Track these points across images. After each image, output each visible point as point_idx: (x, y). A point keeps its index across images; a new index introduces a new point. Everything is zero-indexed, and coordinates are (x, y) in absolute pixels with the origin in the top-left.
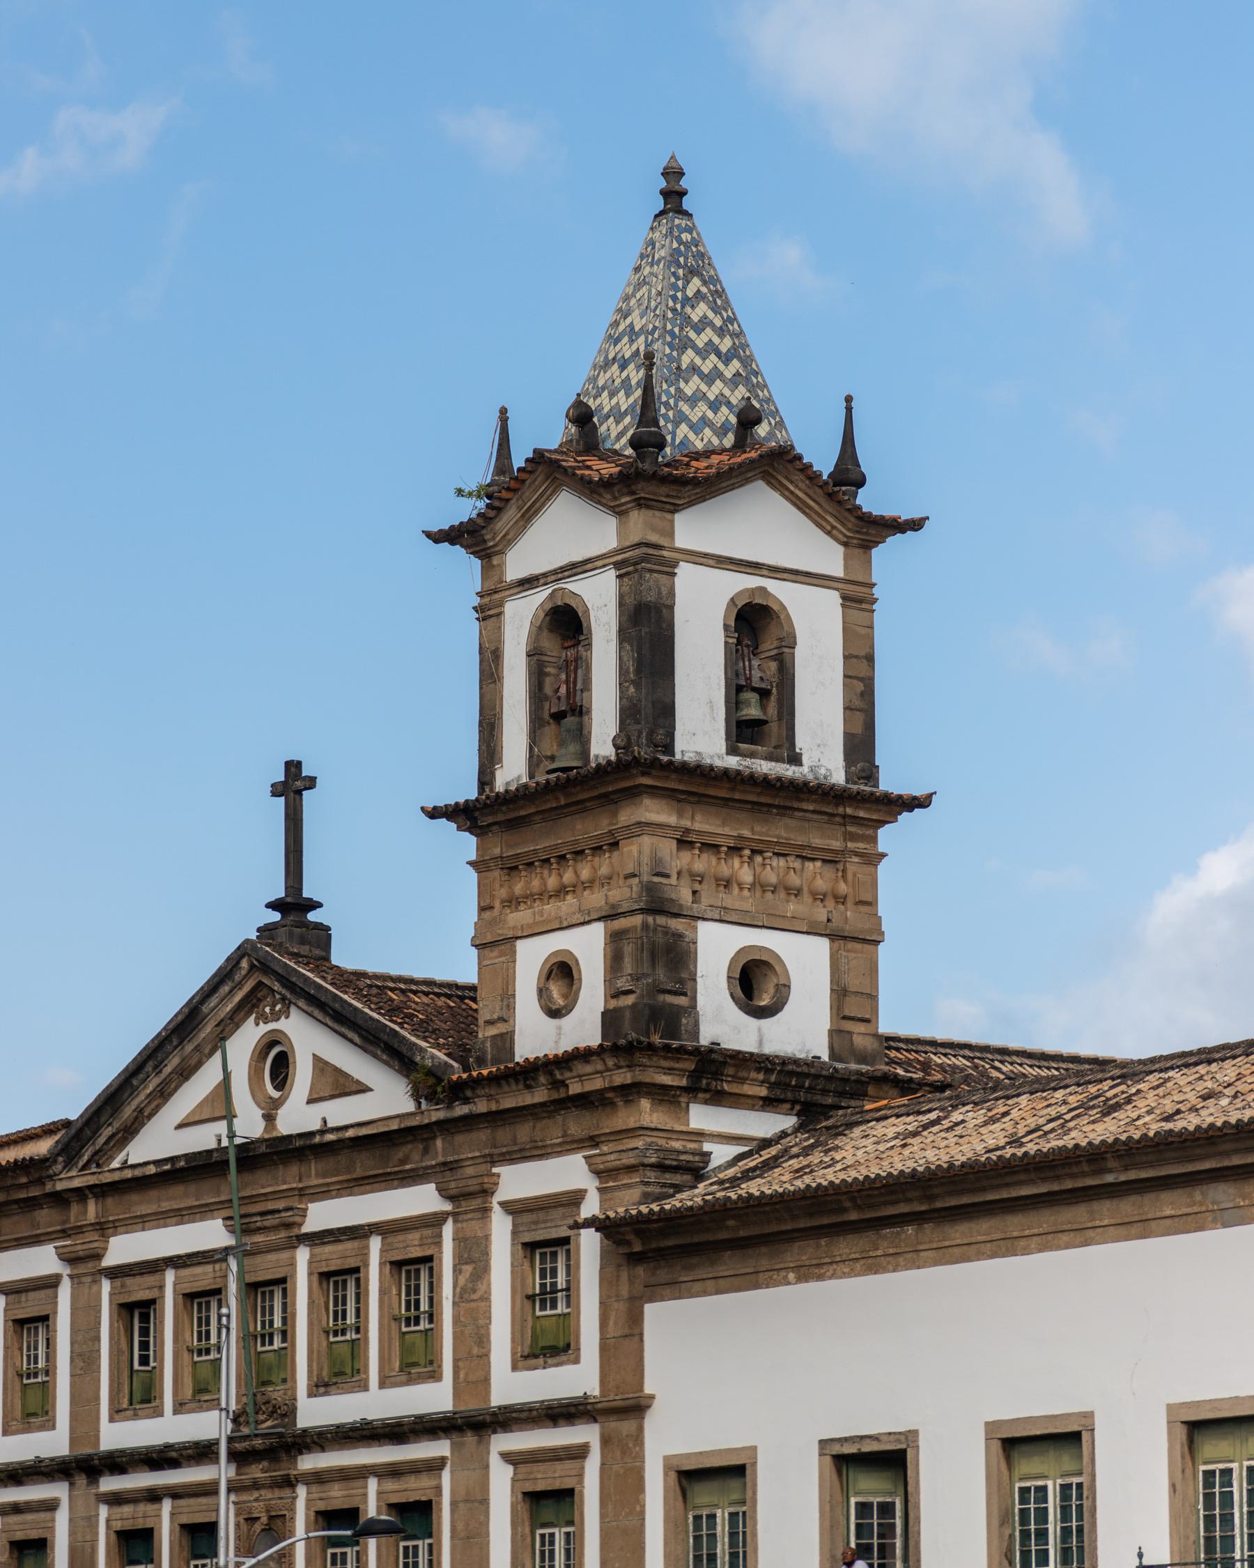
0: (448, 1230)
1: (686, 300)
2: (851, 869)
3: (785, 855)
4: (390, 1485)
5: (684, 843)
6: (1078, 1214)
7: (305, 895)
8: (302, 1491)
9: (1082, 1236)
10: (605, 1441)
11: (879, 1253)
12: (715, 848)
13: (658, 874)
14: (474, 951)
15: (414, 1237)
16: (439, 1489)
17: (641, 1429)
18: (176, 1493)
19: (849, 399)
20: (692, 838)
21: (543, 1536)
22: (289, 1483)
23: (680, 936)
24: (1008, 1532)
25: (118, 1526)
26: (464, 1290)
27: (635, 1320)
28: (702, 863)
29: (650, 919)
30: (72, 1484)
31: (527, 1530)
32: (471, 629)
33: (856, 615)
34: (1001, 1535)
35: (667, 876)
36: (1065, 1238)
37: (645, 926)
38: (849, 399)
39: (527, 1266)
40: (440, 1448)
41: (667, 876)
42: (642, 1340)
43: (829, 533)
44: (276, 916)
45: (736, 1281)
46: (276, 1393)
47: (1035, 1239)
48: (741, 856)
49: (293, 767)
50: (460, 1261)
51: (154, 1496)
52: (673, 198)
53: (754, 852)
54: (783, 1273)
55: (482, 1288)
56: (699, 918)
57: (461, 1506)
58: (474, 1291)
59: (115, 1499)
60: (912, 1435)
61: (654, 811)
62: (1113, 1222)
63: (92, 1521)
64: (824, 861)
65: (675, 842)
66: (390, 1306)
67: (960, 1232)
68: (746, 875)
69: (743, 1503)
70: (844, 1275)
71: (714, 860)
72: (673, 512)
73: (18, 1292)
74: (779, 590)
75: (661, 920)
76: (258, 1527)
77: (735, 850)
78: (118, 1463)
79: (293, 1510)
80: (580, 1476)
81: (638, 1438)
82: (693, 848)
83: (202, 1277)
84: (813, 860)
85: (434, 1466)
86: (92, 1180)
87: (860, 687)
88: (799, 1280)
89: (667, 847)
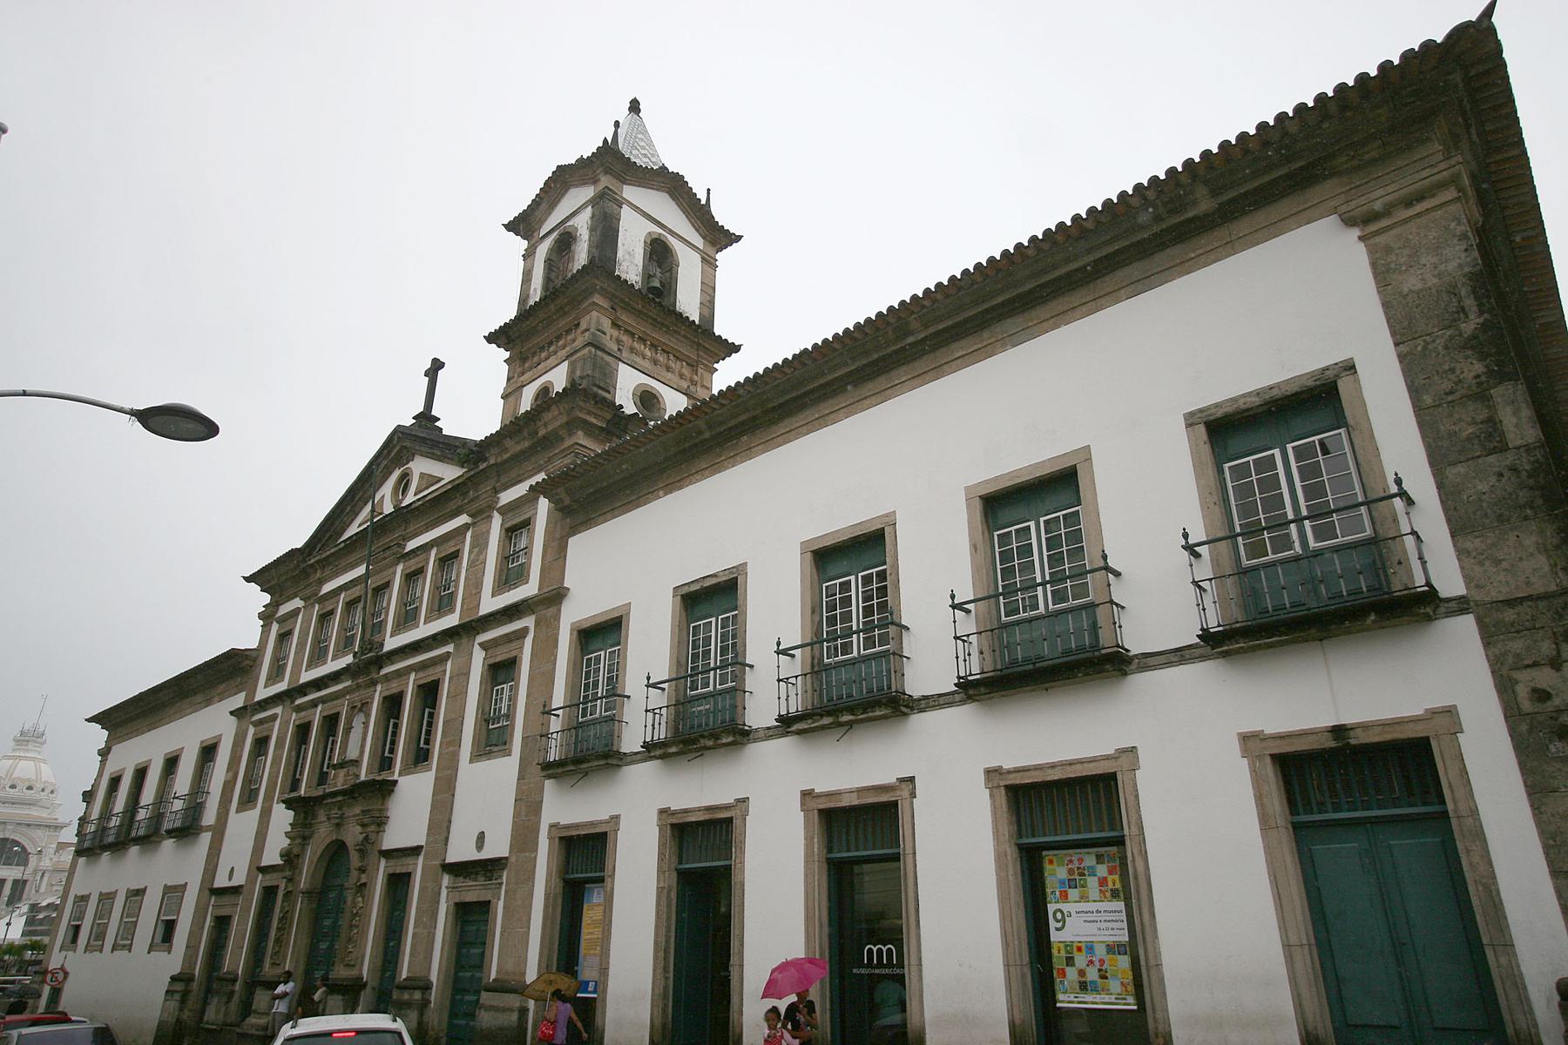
0: (469, 534)
1: (636, 137)
2: (700, 371)
3: (668, 353)
4: (421, 674)
5: (615, 325)
6: (882, 382)
7: (433, 413)
8: (379, 688)
9: (883, 395)
10: (537, 623)
11: (723, 458)
12: (632, 335)
13: (599, 330)
14: (502, 401)
15: (452, 543)
16: (445, 671)
17: (560, 610)
18: (323, 700)
19: (709, 190)
20: (620, 324)
21: (497, 690)
22: (374, 683)
23: (607, 364)
24: (817, 618)
25: (297, 723)
26: (473, 562)
27: (563, 549)
28: (625, 338)
29: (593, 350)
30: (284, 706)
31: (489, 688)
32: (520, 265)
33: (706, 267)
34: (812, 621)
35: (605, 334)
36: (867, 402)
37: (590, 352)
38: (709, 190)
39: (507, 542)
40: (450, 648)
41: (605, 334)
42: (565, 559)
43: (697, 230)
44: (414, 421)
45: (624, 507)
46: (377, 638)
47: (842, 411)
48: (645, 345)
49: (435, 361)
50: (472, 547)
51: (314, 704)
52: (635, 107)
53: (652, 345)
54: (655, 493)
55: (482, 557)
56: (620, 360)
57: (454, 678)
58: (477, 560)
59: (299, 709)
60: (742, 567)
61: (598, 299)
62: (910, 377)
63: (288, 722)
64: (688, 364)
65: (610, 321)
66: (436, 581)
67: (782, 428)
68: (648, 353)
69: (619, 644)
70: (698, 481)
71: (631, 341)
72: (624, 183)
73: (283, 622)
74: (672, 240)
75: (599, 353)
76: (357, 710)
77: (642, 340)
78: (302, 690)
79: (372, 698)
80: (522, 648)
81: (557, 617)
82: (620, 330)
83: (356, 591)
84: (683, 361)
85: (444, 659)
86: (317, 558)
87: (708, 298)
88: (666, 494)
89: (606, 323)
